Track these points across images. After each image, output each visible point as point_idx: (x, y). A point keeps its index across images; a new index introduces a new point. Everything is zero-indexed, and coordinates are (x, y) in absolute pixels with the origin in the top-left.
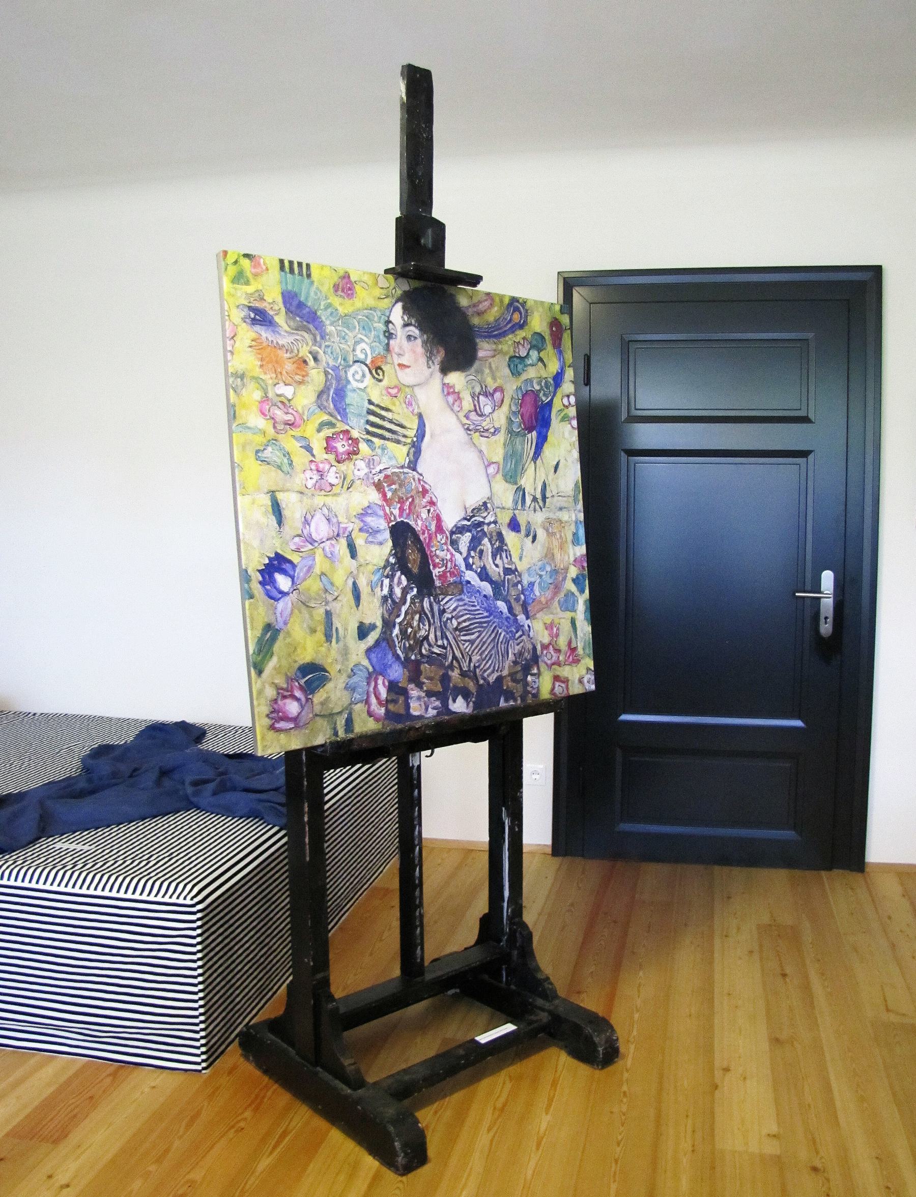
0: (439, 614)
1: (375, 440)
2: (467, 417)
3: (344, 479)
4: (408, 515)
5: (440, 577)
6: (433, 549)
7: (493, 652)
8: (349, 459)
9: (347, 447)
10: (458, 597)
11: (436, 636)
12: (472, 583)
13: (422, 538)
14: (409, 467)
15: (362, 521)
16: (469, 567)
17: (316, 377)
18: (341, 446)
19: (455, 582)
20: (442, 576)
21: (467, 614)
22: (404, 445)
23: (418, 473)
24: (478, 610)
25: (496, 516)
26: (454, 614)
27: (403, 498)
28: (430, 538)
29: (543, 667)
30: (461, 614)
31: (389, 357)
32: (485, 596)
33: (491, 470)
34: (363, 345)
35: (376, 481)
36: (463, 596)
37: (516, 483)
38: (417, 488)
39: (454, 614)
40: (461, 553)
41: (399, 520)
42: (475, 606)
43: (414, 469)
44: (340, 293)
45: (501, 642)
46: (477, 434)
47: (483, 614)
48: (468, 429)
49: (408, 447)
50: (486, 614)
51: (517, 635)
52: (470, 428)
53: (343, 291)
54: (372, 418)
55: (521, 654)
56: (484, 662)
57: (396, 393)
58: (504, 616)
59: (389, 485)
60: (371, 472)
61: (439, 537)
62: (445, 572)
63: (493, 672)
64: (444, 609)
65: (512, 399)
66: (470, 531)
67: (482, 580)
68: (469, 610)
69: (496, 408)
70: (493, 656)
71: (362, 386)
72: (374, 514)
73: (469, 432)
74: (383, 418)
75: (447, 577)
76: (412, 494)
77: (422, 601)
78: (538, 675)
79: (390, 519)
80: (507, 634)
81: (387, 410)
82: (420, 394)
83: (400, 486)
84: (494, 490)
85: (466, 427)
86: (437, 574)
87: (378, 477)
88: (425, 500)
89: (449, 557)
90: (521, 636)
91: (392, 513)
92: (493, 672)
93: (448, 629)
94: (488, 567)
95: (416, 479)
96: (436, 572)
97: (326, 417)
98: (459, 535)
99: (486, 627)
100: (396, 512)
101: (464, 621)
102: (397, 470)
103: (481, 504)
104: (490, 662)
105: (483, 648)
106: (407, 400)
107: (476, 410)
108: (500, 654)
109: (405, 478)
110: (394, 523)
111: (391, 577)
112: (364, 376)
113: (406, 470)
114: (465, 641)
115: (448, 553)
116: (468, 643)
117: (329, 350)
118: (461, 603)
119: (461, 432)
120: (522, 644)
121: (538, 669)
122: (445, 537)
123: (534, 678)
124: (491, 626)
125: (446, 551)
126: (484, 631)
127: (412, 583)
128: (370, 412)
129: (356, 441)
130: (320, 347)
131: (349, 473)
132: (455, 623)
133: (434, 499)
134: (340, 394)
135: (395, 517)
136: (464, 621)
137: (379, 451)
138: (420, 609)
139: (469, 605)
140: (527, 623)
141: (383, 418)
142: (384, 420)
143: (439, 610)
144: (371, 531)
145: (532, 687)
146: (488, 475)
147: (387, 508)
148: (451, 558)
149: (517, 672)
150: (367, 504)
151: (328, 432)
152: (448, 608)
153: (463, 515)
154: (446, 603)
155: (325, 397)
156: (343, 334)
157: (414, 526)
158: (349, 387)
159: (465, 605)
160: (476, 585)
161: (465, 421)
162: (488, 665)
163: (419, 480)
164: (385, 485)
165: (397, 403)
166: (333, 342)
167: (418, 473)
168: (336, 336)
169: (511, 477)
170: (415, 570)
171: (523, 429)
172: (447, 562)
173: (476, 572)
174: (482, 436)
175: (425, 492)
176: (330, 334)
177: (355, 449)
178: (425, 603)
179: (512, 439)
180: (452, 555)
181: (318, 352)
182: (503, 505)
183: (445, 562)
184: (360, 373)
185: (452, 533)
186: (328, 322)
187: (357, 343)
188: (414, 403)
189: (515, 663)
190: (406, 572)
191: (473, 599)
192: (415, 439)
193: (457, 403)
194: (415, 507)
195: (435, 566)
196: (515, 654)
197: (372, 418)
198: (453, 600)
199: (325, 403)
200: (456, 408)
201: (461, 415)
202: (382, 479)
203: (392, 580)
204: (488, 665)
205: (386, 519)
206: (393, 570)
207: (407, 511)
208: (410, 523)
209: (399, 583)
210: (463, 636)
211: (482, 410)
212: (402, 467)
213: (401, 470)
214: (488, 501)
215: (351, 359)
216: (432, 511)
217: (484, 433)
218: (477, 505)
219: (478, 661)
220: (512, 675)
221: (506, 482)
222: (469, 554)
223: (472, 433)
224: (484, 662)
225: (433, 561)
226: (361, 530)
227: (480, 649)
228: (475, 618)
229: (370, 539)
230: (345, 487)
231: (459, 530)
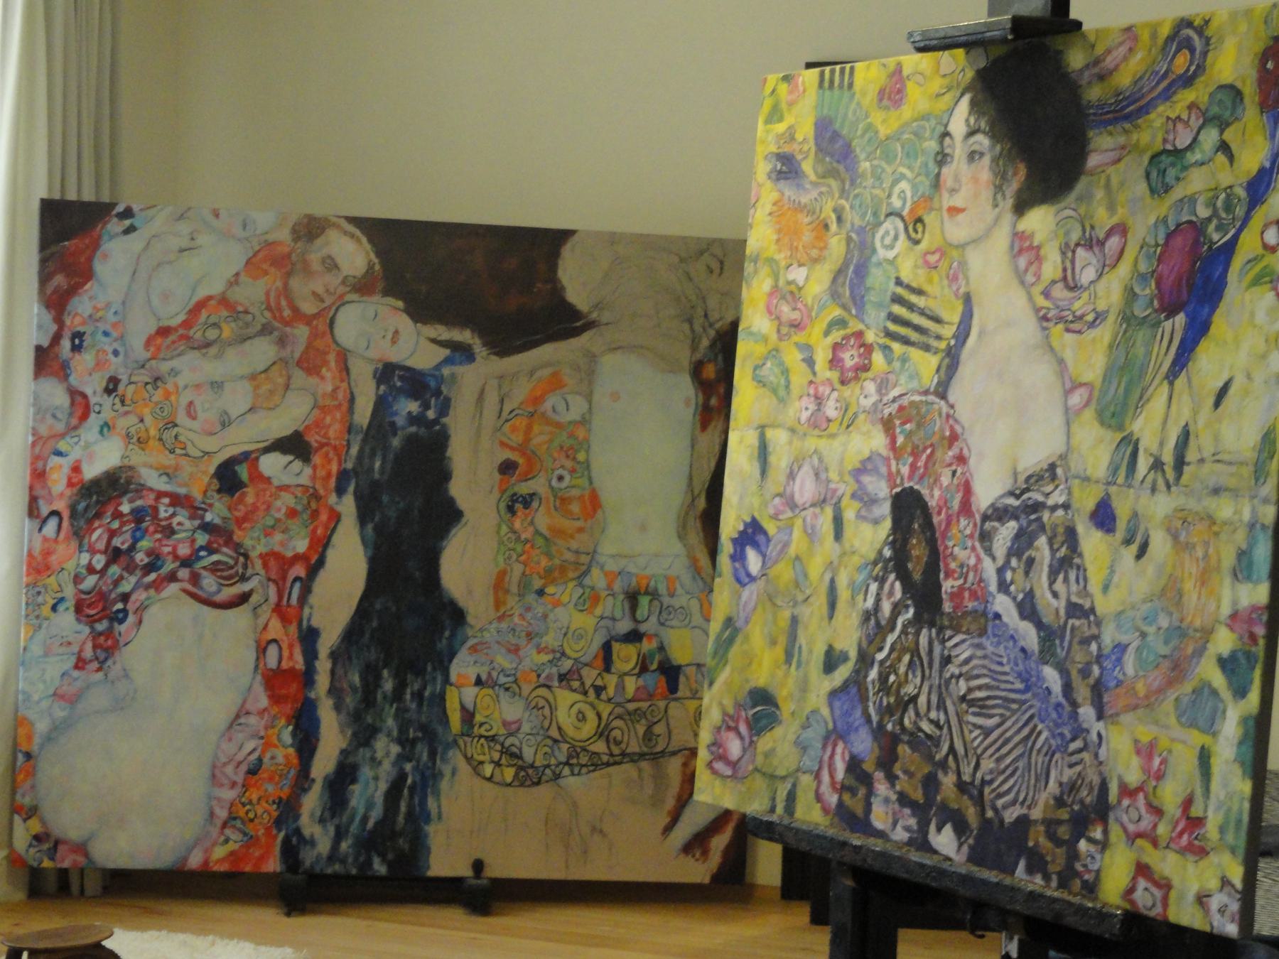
0: (941, 663)
2: (1046, 294)
3: (846, 410)
4: (922, 478)
5: (953, 596)
6: (950, 544)
7: (1021, 764)
8: (857, 378)
9: (856, 360)
10: (976, 641)
11: (929, 702)
12: (1005, 619)
13: (936, 520)
14: (936, 393)
15: (858, 481)
16: (1003, 587)
17: (836, 246)
18: (850, 358)
19: (976, 611)
20: (957, 595)
21: (985, 675)
22: (935, 353)
23: (947, 402)
24: (1005, 674)
25: (1070, 493)
26: (965, 669)
27: (918, 446)
28: (949, 523)
29: (1116, 833)
30: (976, 672)
31: (936, 199)
32: (1023, 650)
33: (1076, 399)
34: (904, 185)
35: (886, 416)
36: (984, 640)
37: (1120, 427)
38: (942, 430)
39: (965, 669)
40: (994, 559)
41: (907, 485)
42: (1001, 664)
43: (943, 396)
44: (885, 102)
45: (1039, 751)
46: (1061, 326)
47: (1012, 683)
48: (1045, 318)
49: (940, 356)
50: (1019, 686)
51: (1074, 746)
52: (1049, 316)
53: (889, 98)
54: (898, 310)
55: (1073, 787)
56: (1001, 778)
57: (938, 261)
58: (1053, 700)
59: (904, 423)
60: (881, 400)
61: (963, 522)
62: (961, 588)
63: (1014, 803)
64: (949, 656)
65: (1142, 247)
66: (1016, 518)
67: (1023, 616)
68: (990, 670)
69: (1107, 269)
70: (1018, 773)
71: (891, 255)
72: (876, 471)
73: (1045, 324)
74: (911, 307)
75: (963, 598)
76: (935, 439)
77: (917, 634)
78: (1104, 845)
79: (895, 481)
80: (1054, 736)
81: (919, 292)
82: (975, 260)
83: (919, 425)
84: (1075, 441)
85: (1041, 313)
86: (949, 590)
87: (890, 410)
88: (950, 453)
89: (972, 561)
90: (1080, 751)
91: (898, 472)
92: (1014, 803)
93: (950, 695)
94: (1038, 593)
95: (944, 415)
96: (948, 586)
97: (837, 312)
98: (996, 524)
99: (1018, 710)
100: (905, 470)
101: (980, 688)
102: (917, 398)
103: (1045, 467)
104: (1011, 782)
105: (1004, 751)
106: (952, 272)
107: (1065, 278)
108: (1033, 773)
109: (928, 411)
110: (898, 489)
112: (896, 238)
113: (931, 398)
114: (976, 726)
115: (973, 555)
116: (977, 732)
117: (857, 202)
118: (979, 653)
119: (1028, 327)
120: (1078, 768)
121: (1106, 832)
122: (971, 525)
123: (1092, 849)
124: (1026, 711)
125: (968, 551)
126: (1009, 717)
127: (908, 599)
128: (898, 300)
129: (869, 349)
130: (847, 199)
131: (853, 400)
132: (963, 686)
133: (965, 452)
134: (861, 271)
135: (902, 479)
136: (980, 688)
137: (897, 365)
138: (912, 646)
139: (992, 661)
140: (1099, 726)
141: (911, 307)
142: (913, 311)
143: (942, 655)
144: (866, 499)
145: (1085, 866)
146: (1067, 410)
147: (893, 463)
148: (976, 565)
149: (1060, 822)
150: (866, 454)
151: (836, 336)
152: (957, 656)
153: (1008, 486)
154: (956, 645)
155: (840, 280)
156: (880, 170)
157: (927, 499)
158: (874, 259)
159: (985, 657)
160: (1011, 625)
161: (1041, 301)
162: (1006, 787)
163: (948, 416)
164: (898, 422)
165: (936, 278)
166: (865, 187)
167: (947, 402)
168: (869, 175)
169: (1113, 415)
170: (917, 577)
171: (1156, 311)
172: (967, 572)
173: (1014, 599)
174: (1068, 330)
175: (954, 438)
176: (863, 176)
177: (866, 362)
178: (921, 638)
179: (1128, 334)
180: (979, 559)
181: (843, 208)
182: (1088, 473)
183: (965, 570)
184: (892, 233)
185: (985, 518)
186: (862, 156)
188: (961, 276)
189: (1060, 802)
190: (904, 576)
191: (1001, 650)
192: (953, 342)
193: (1033, 269)
194: (934, 464)
195: (947, 575)
196: (1061, 784)
197: (898, 310)
198: (968, 643)
199: (840, 290)
201: (1037, 290)
202: (894, 413)
203: (881, 588)
204: (1006, 787)
205: (889, 480)
206: (885, 569)
207: (922, 470)
208: (923, 492)
209: (891, 594)
210: (975, 714)
211: (1077, 277)
212: (926, 393)
213: (924, 398)
214: (1058, 463)
215: (884, 210)
216: (959, 471)
217: (1074, 323)
218: (1038, 469)
219: (991, 772)
220: (1050, 825)
221: (1102, 423)
222: (1007, 562)
223: (1050, 324)
224: (1001, 778)
225: (947, 565)
226: (853, 496)
227: (998, 749)
228: (998, 688)
229: (863, 513)
230: (845, 424)
231: (999, 513)
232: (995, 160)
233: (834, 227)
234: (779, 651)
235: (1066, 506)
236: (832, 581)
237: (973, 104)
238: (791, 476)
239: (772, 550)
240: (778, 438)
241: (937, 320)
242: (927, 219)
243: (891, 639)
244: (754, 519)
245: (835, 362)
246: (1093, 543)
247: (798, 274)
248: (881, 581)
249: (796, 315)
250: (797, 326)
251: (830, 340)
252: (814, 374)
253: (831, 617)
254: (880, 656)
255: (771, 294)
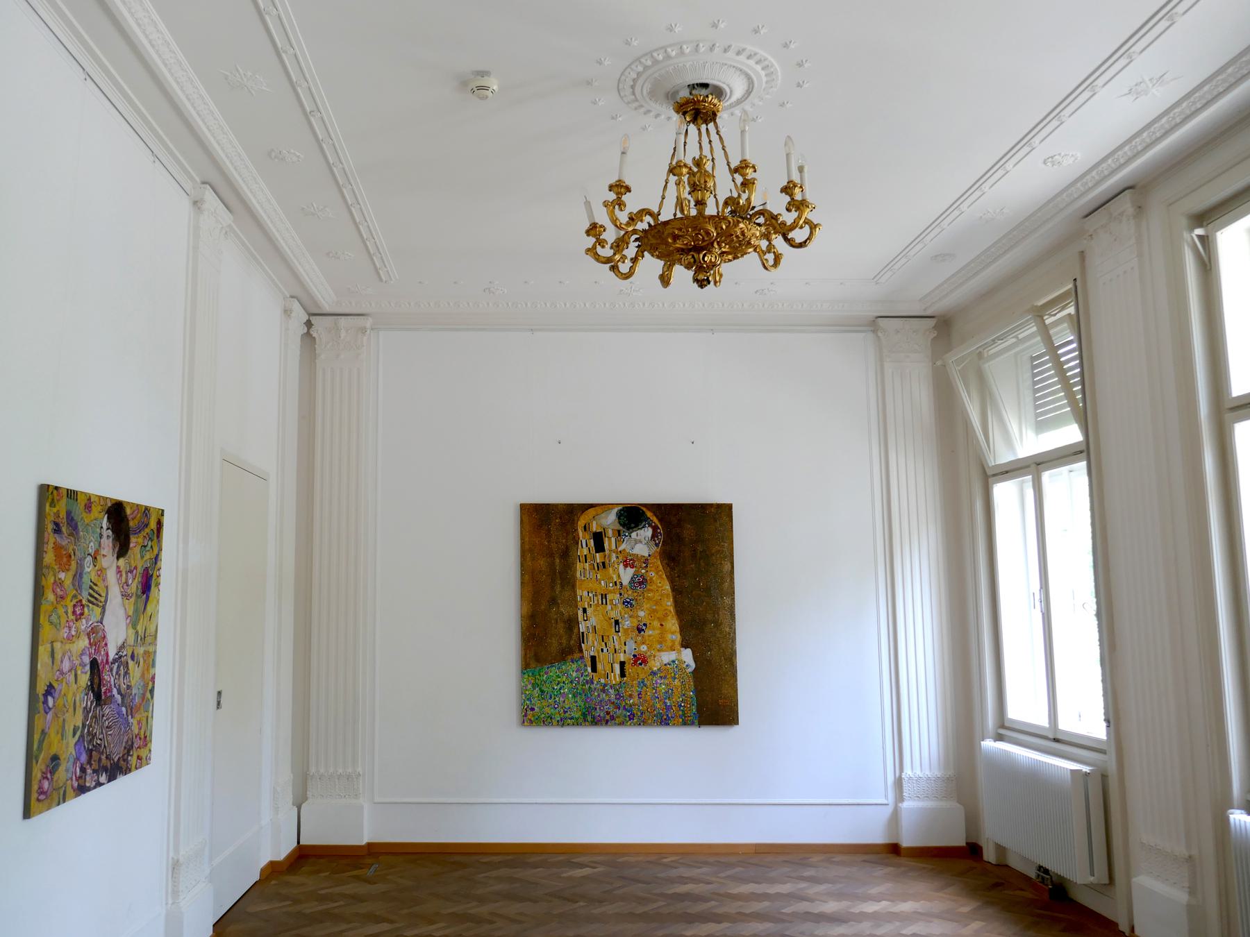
1: (90, 605)
34: (92, 544)
96: (103, 690)
102: (96, 624)
111: (87, 694)
119: (120, 596)
128: (91, 588)
141: (94, 590)
150: (83, 647)
187: (90, 542)
200: (120, 582)
206: (89, 691)
215: (87, 553)
232: (113, 540)
233: (73, 557)
234: (60, 735)
235: (126, 655)
236: (75, 700)
237: (108, 518)
238: (62, 662)
239: (56, 695)
240: (57, 646)
241: (99, 595)
242: (98, 557)
243: (90, 715)
244: (50, 683)
245: (74, 613)
246: (131, 663)
247: (62, 575)
248: (87, 694)
249: (61, 593)
250: (62, 598)
251: (72, 604)
252: (68, 617)
253: (74, 714)
254: (87, 723)
255: (54, 583)
